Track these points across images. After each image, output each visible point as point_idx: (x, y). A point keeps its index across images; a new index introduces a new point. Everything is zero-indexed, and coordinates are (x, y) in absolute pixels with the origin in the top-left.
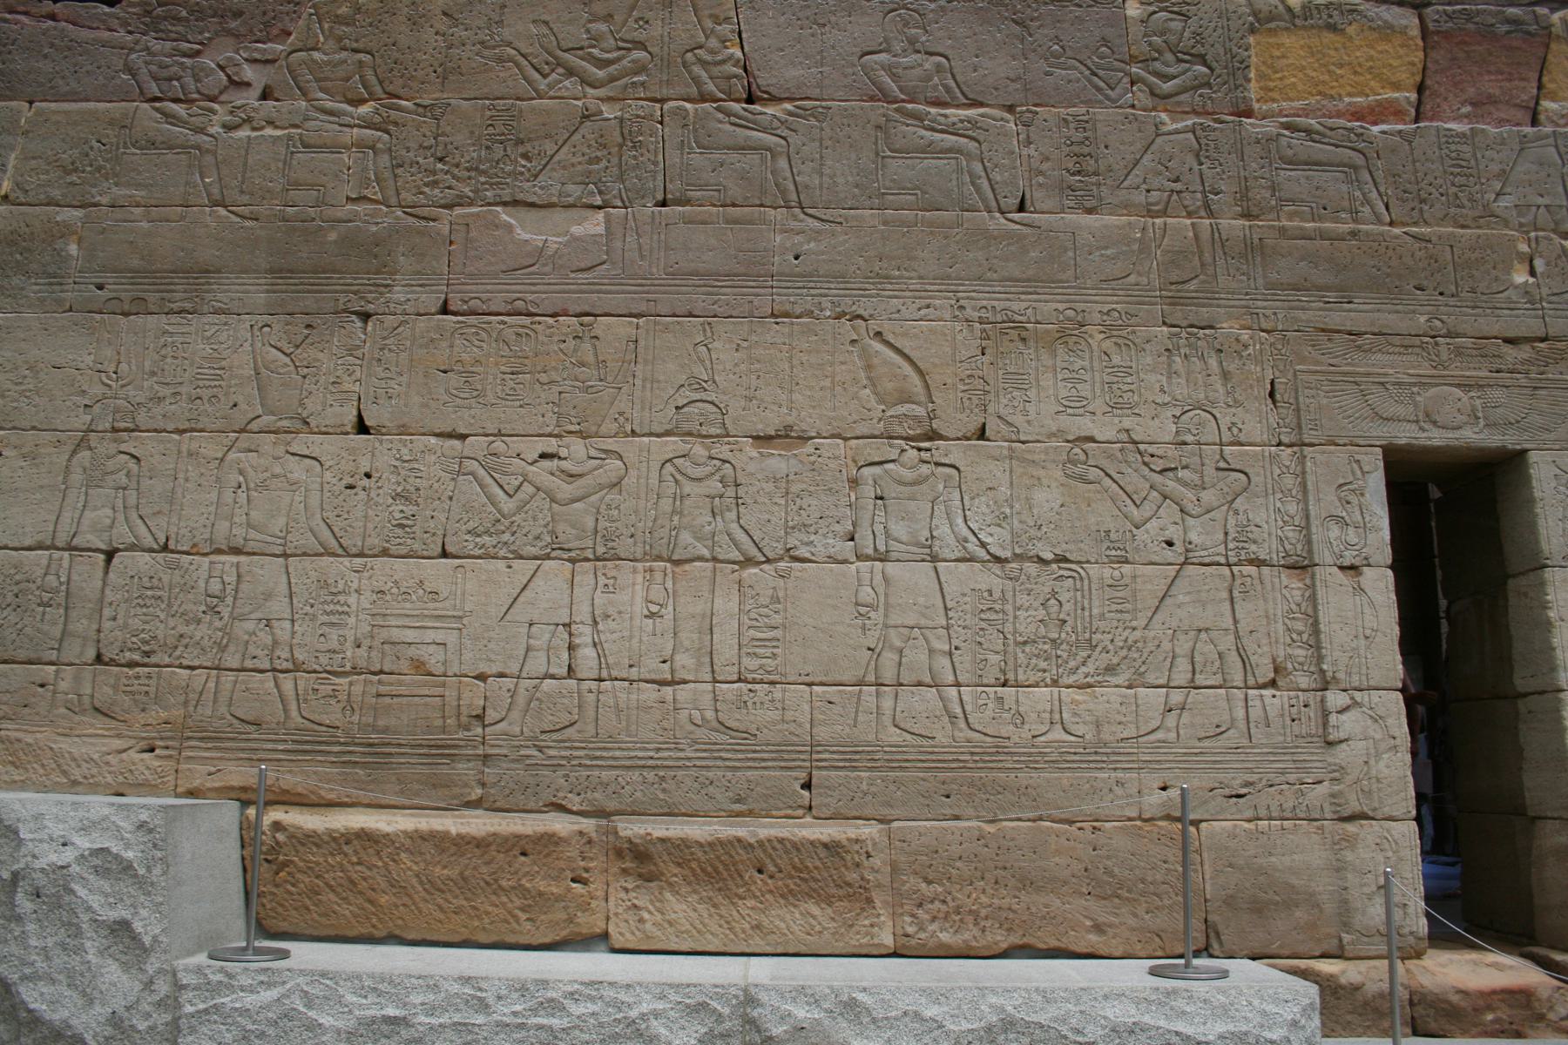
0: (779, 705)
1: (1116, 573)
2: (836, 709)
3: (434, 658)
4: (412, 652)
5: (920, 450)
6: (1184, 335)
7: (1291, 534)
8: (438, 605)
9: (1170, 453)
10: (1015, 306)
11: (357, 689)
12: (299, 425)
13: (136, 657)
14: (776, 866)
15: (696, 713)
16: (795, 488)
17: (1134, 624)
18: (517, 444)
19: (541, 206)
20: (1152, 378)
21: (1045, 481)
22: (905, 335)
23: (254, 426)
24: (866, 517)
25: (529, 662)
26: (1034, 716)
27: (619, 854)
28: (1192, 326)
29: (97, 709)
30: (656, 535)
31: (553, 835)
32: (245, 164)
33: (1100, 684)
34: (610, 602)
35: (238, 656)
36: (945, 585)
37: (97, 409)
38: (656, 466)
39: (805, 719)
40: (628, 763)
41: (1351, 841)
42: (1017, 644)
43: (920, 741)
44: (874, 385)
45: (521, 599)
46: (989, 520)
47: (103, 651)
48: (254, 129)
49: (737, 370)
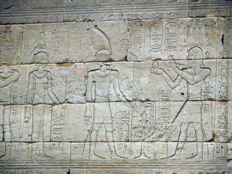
1: (165, 104)
2: (78, 149)
5: (107, 65)
6: (195, 20)
7: (223, 90)
9: (185, 63)
10: (139, 14)
15: (38, 152)
16: (69, 80)
17: (169, 121)
20: (182, 36)
21: (144, 74)
22: (104, 26)
26: (135, 151)
28: (198, 17)
30: (28, 96)
33: (157, 141)
34: (15, 118)
36: (112, 110)
39: (69, 153)
42: (132, 128)
43: (101, 159)
46: (126, 88)
49: (52, 41)
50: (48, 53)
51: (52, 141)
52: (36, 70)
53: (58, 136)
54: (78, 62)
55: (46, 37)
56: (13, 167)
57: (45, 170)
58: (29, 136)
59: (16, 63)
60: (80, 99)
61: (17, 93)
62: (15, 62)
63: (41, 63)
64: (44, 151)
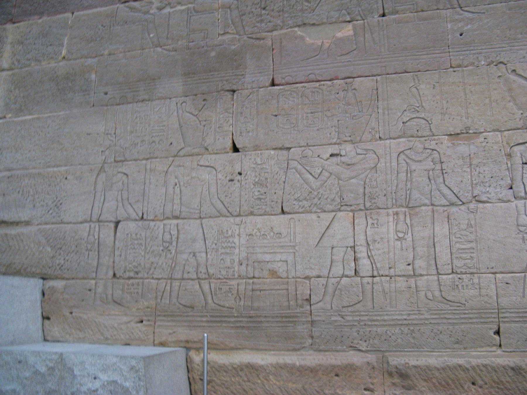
0: (477, 287)
3: (281, 268)
4: (270, 266)
8: (282, 240)
11: (242, 287)
12: (203, 150)
13: (132, 274)
14: (483, 380)
18: (318, 150)
19: (318, 25)
23: (181, 153)
24: (518, 175)
25: (333, 269)
27: (391, 374)
29: (115, 302)
31: (353, 364)
32: (168, 25)
35: (180, 273)
37: (107, 153)
38: (395, 156)
39: (493, 293)
40: (392, 323)
44: (515, 100)
45: (326, 234)
47: (116, 272)
48: (172, 8)
50: (429, 119)
51: (457, 273)
52: (410, 149)
53: (466, 264)
54: (489, 130)
55: (421, 93)
56: (381, 323)
57: (447, 327)
58: (409, 265)
59: (369, 139)
60: (503, 194)
61: (377, 189)
62: (367, 136)
63: (418, 137)
64: (441, 291)
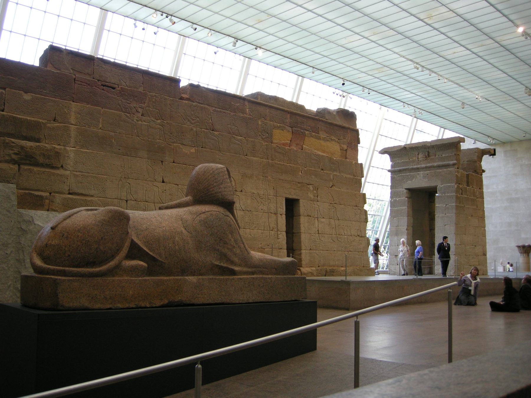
41: (280, 252)
